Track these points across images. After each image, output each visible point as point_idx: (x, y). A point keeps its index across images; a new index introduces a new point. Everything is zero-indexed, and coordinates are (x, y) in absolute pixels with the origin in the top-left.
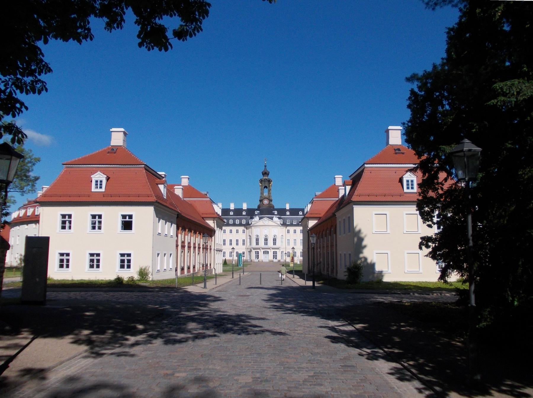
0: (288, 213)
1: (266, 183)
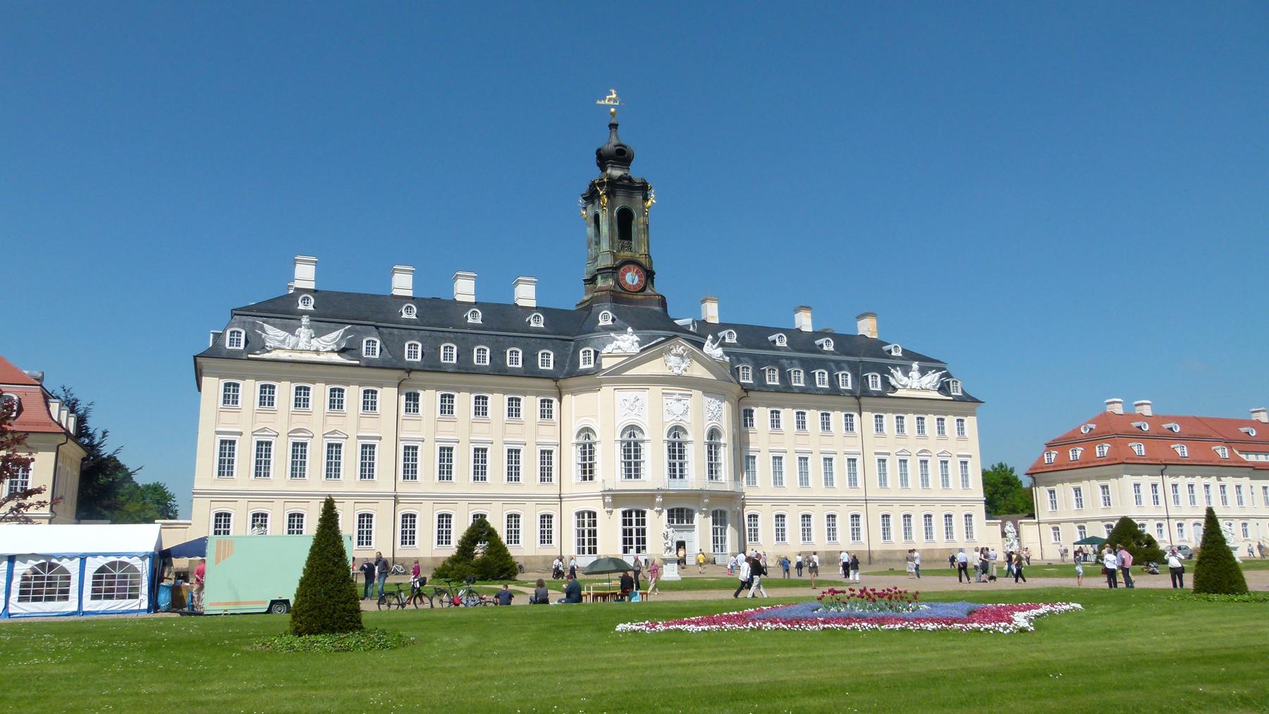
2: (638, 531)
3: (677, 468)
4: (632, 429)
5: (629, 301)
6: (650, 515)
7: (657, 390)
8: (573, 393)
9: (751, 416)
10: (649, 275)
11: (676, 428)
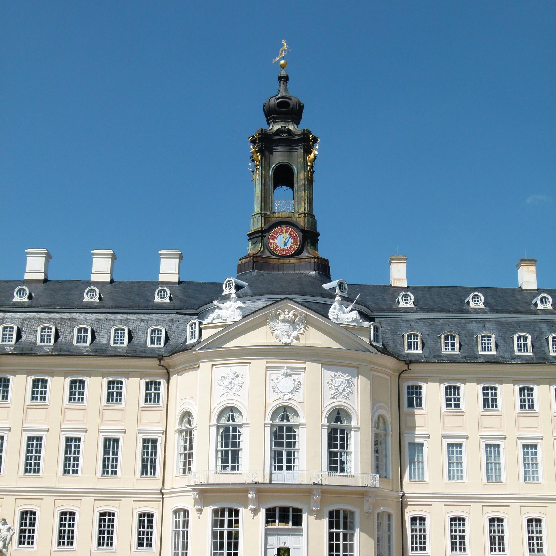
0: (406, 302)
1: (282, 141)
2: (230, 533)
3: (285, 457)
4: (230, 411)
5: (280, 267)
6: (244, 514)
7: (259, 364)
8: (178, 373)
9: (419, 393)
10: (310, 237)
11: (285, 408)
